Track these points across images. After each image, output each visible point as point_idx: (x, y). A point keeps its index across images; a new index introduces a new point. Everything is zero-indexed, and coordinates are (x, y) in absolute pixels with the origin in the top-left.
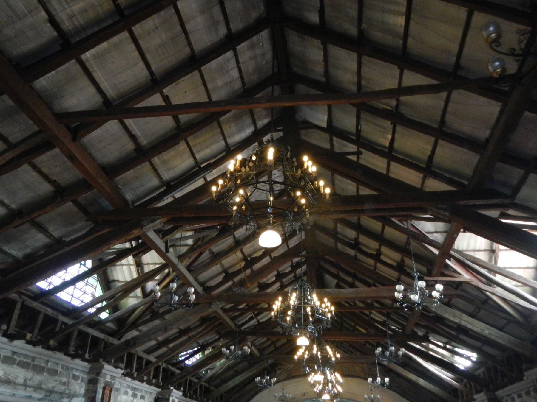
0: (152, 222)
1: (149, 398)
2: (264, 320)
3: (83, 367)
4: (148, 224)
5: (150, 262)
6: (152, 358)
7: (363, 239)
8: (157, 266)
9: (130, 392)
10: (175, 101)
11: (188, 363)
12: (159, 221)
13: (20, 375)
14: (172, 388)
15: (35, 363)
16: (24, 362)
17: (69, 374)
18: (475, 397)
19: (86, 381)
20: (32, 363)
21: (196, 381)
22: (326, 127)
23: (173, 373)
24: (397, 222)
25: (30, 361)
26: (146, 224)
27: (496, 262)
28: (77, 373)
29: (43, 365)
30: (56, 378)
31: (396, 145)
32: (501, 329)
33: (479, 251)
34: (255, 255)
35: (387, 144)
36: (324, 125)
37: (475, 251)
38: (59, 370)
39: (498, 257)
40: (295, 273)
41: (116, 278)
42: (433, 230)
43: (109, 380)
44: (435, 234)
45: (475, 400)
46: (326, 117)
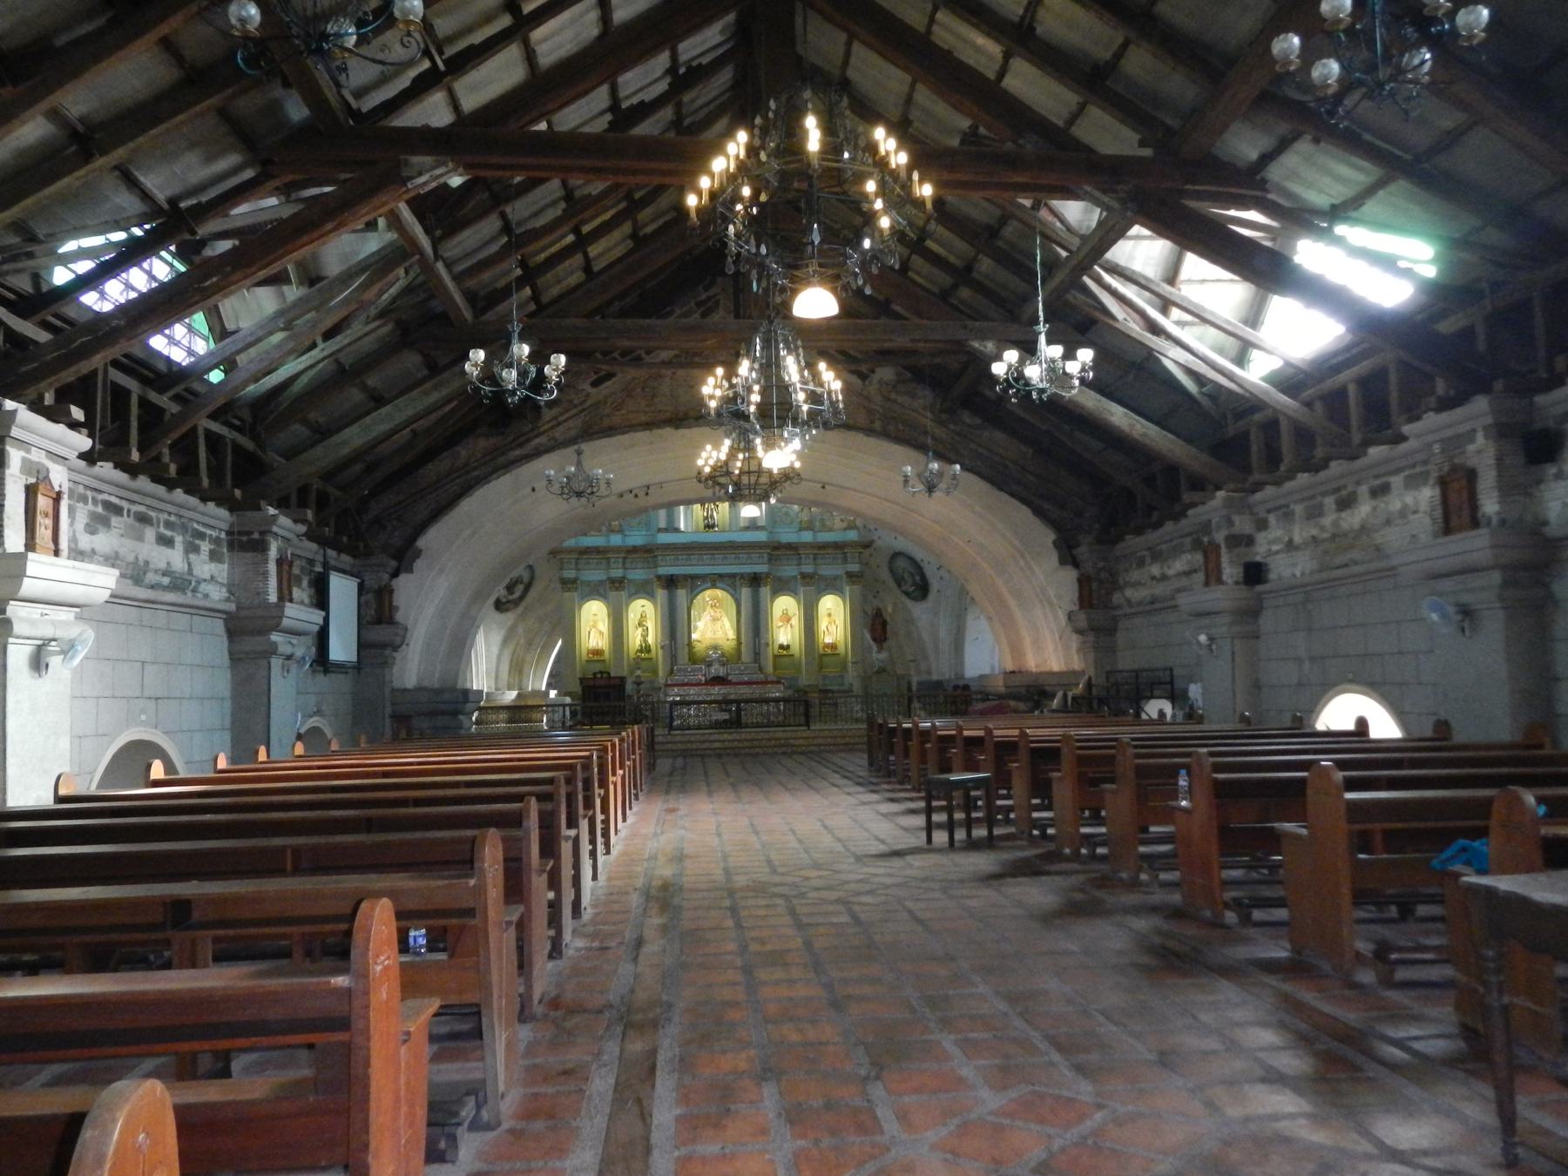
18: (1407, 429)
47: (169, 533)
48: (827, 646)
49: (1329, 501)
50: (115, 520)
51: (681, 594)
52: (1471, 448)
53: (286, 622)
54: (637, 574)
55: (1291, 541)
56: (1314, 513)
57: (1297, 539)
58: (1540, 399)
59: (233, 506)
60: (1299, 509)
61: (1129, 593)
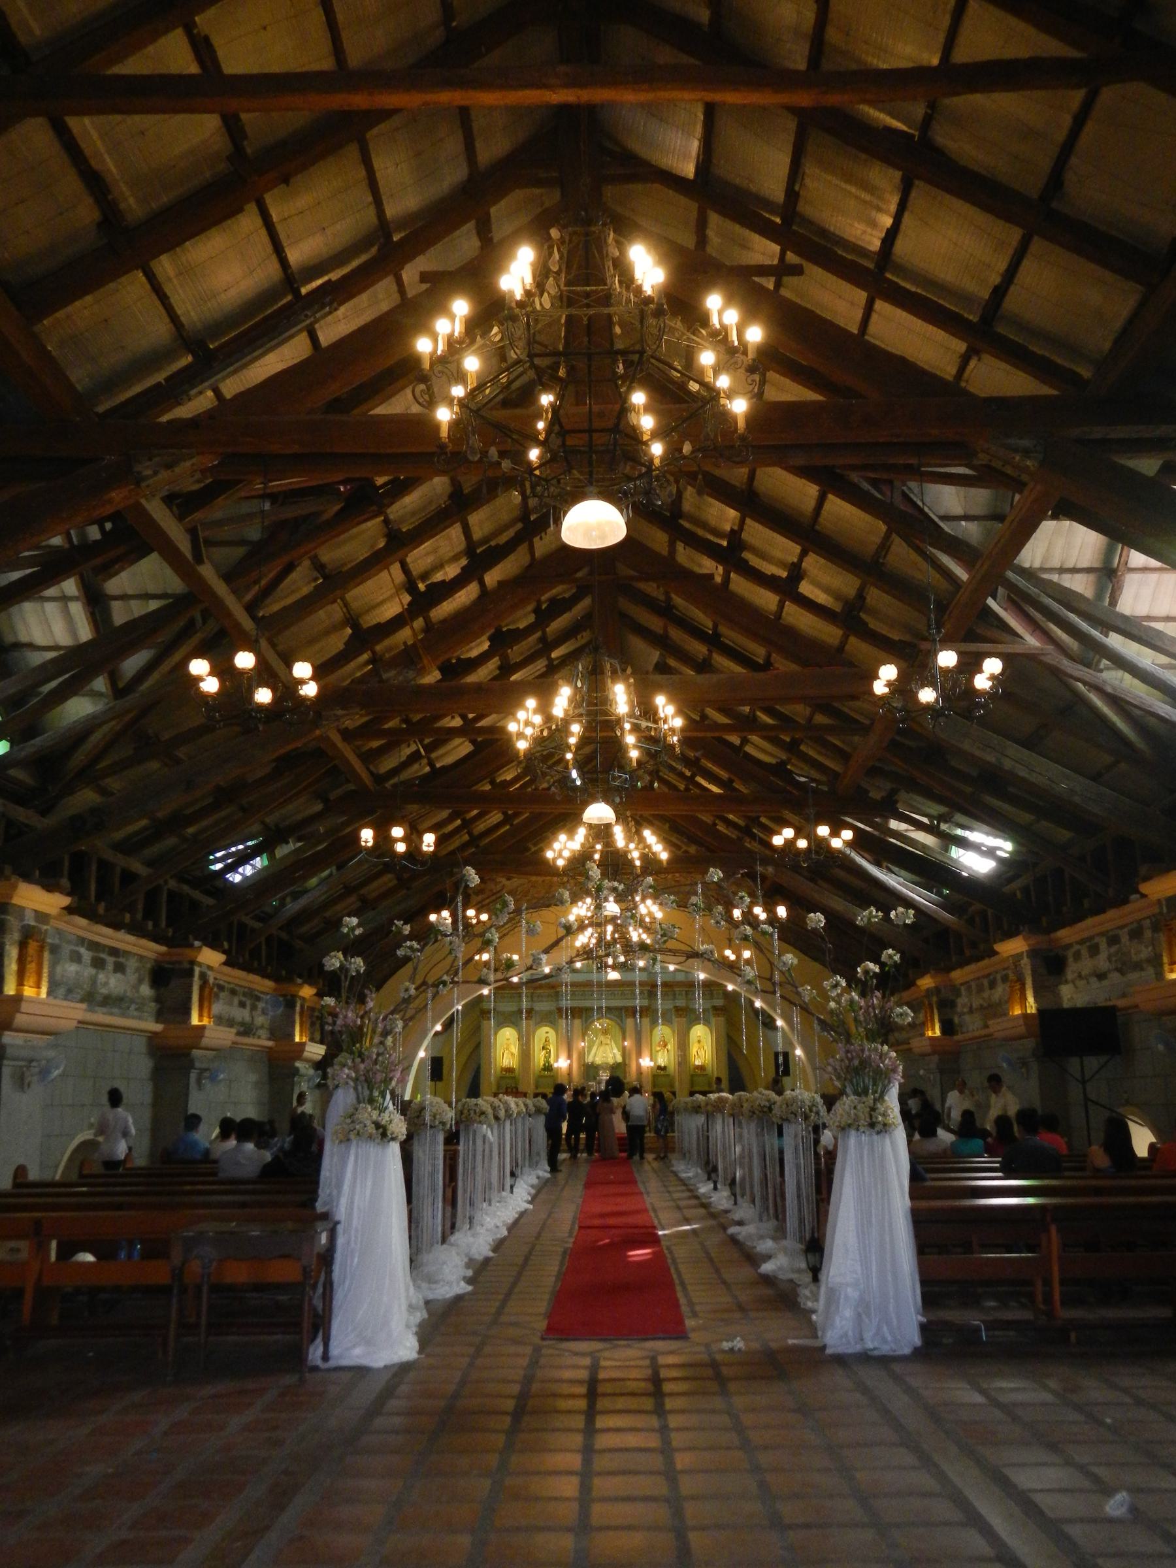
0: (169, 466)
2: (449, 760)
4: (156, 473)
5: (130, 592)
6: (137, 866)
7: (757, 533)
8: (154, 605)
9: (87, 955)
10: (236, 61)
11: (236, 878)
12: (188, 464)
14: (197, 943)
21: (257, 925)
22: (691, 176)
23: (195, 905)
24: (866, 486)
26: (149, 472)
27: (1114, 602)
31: (901, 247)
32: (1096, 777)
33: (1074, 570)
34: (438, 577)
35: (875, 244)
36: (689, 170)
37: (1062, 570)
39: (1121, 588)
40: (544, 633)
41: (23, 638)
42: (958, 510)
43: (33, 923)
44: (963, 523)
45: (996, 953)
46: (695, 145)
47: (244, 999)
48: (698, 1067)
49: (986, 982)
50: (222, 995)
51: (577, 1022)
52: (1022, 962)
53: (306, 1054)
54: (543, 1006)
55: (971, 1007)
56: (980, 989)
57: (974, 1006)
58: (1052, 935)
59: (277, 979)
60: (973, 984)
61: (896, 1034)
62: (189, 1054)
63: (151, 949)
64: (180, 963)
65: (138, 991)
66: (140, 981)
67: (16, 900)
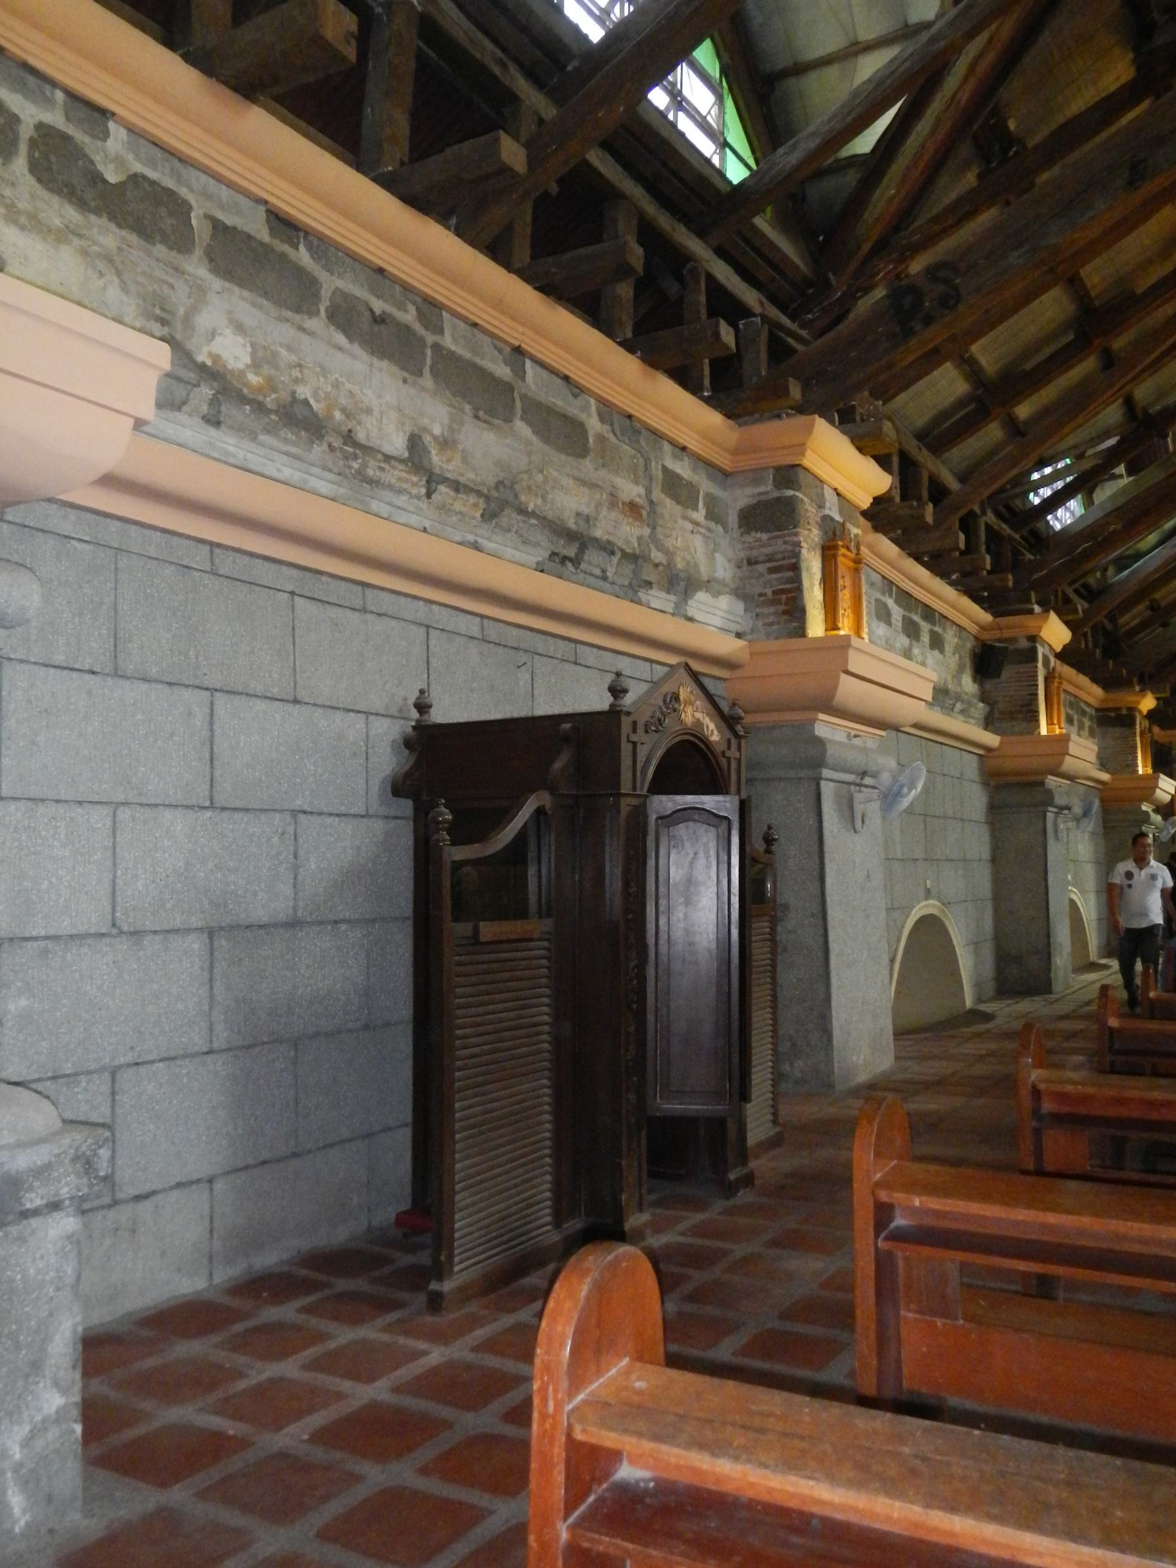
1: (957, 649)
3: (705, 435)
9: (897, 612)
13: (369, 397)
15: (448, 341)
16: (380, 320)
17: (647, 461)
19: (733, 519)
20: (430, 338)
25: (409, 316)
28: (682, 468)
29: (503, 371)
30: (588, 465)
38: (594, 424)
59: (1107, 683)
62: (1042, 784)
63: (971, 614)
64: (1013, 640)
65: (960, 684)
66: (961, 669)
67: (810, 460)
